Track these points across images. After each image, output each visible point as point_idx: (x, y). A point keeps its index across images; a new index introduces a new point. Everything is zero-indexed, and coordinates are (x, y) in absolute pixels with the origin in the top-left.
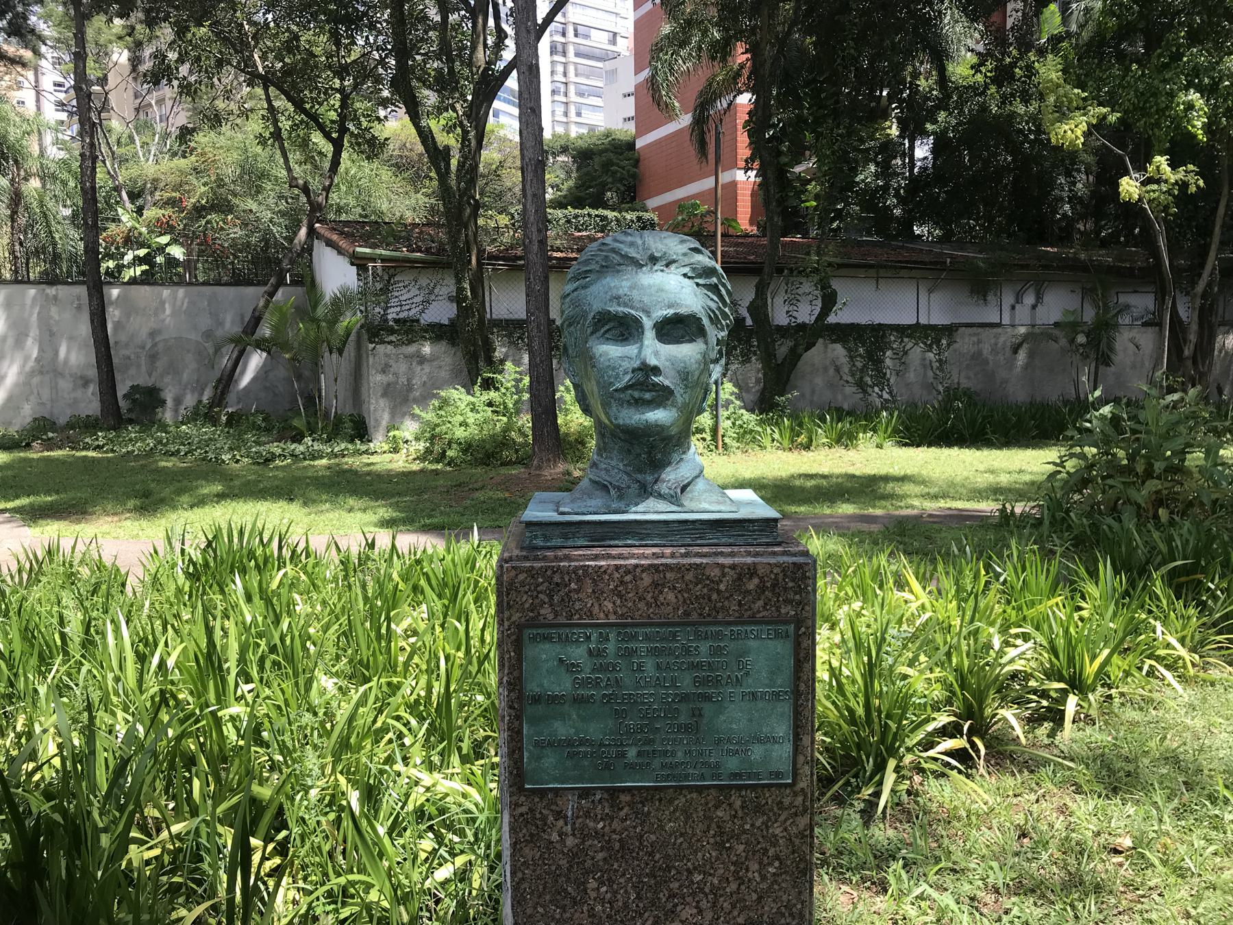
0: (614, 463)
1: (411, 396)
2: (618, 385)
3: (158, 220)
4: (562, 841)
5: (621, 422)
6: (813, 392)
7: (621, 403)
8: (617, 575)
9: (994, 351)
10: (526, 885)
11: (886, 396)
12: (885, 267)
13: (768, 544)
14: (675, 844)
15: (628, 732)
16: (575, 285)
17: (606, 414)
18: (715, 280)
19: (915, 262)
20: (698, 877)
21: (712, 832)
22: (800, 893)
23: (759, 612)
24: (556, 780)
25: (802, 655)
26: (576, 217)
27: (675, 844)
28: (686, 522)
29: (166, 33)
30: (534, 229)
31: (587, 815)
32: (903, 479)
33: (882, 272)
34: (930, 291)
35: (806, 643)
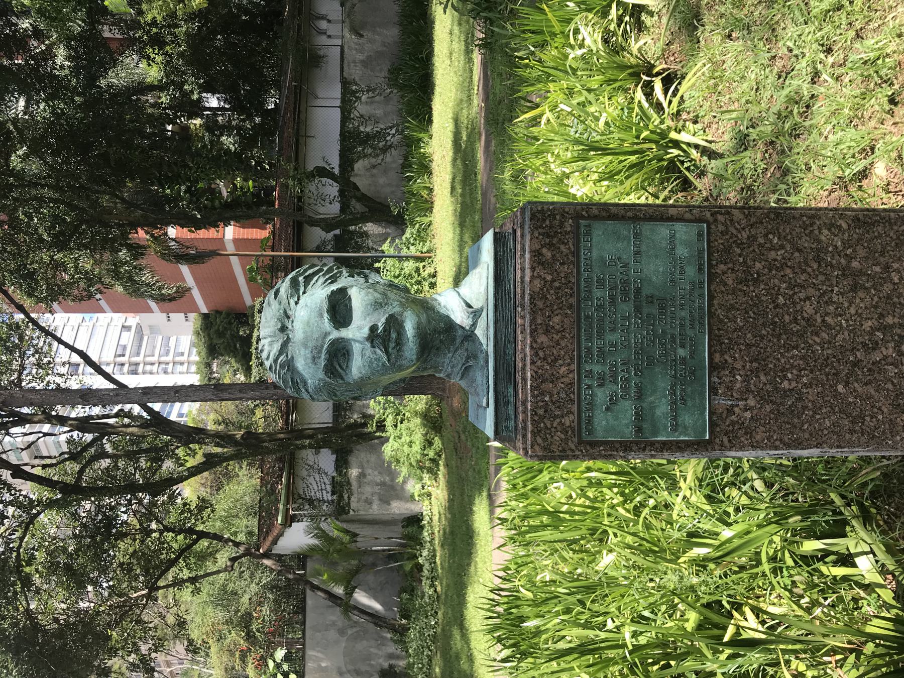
0: (447, 361)
2: (385, 359)
3: (256, 667)
4: (751, 409)
5: (415, 357)
6: (389, 185)
7: (399, 356)
8: (539, 363)
9: (361, 51)
10: (786, 439)
11: (393, 131)
12: (298, 130)
13: (515, 240)
14: (754, 318)
15: (665, 355)
16: (303, 390)
17: (407, 368)
18: (301, 279)
19: (295, 109)
20: (781, 300)
22: (794, 218)
25: (604, 214)
27: (754, 318)
28: (496, 306)
30: (266, 392)
31: (730, 388)
32: (456, 121)
33: (302, 133)
34: (317, 97)
35: (595, 211)
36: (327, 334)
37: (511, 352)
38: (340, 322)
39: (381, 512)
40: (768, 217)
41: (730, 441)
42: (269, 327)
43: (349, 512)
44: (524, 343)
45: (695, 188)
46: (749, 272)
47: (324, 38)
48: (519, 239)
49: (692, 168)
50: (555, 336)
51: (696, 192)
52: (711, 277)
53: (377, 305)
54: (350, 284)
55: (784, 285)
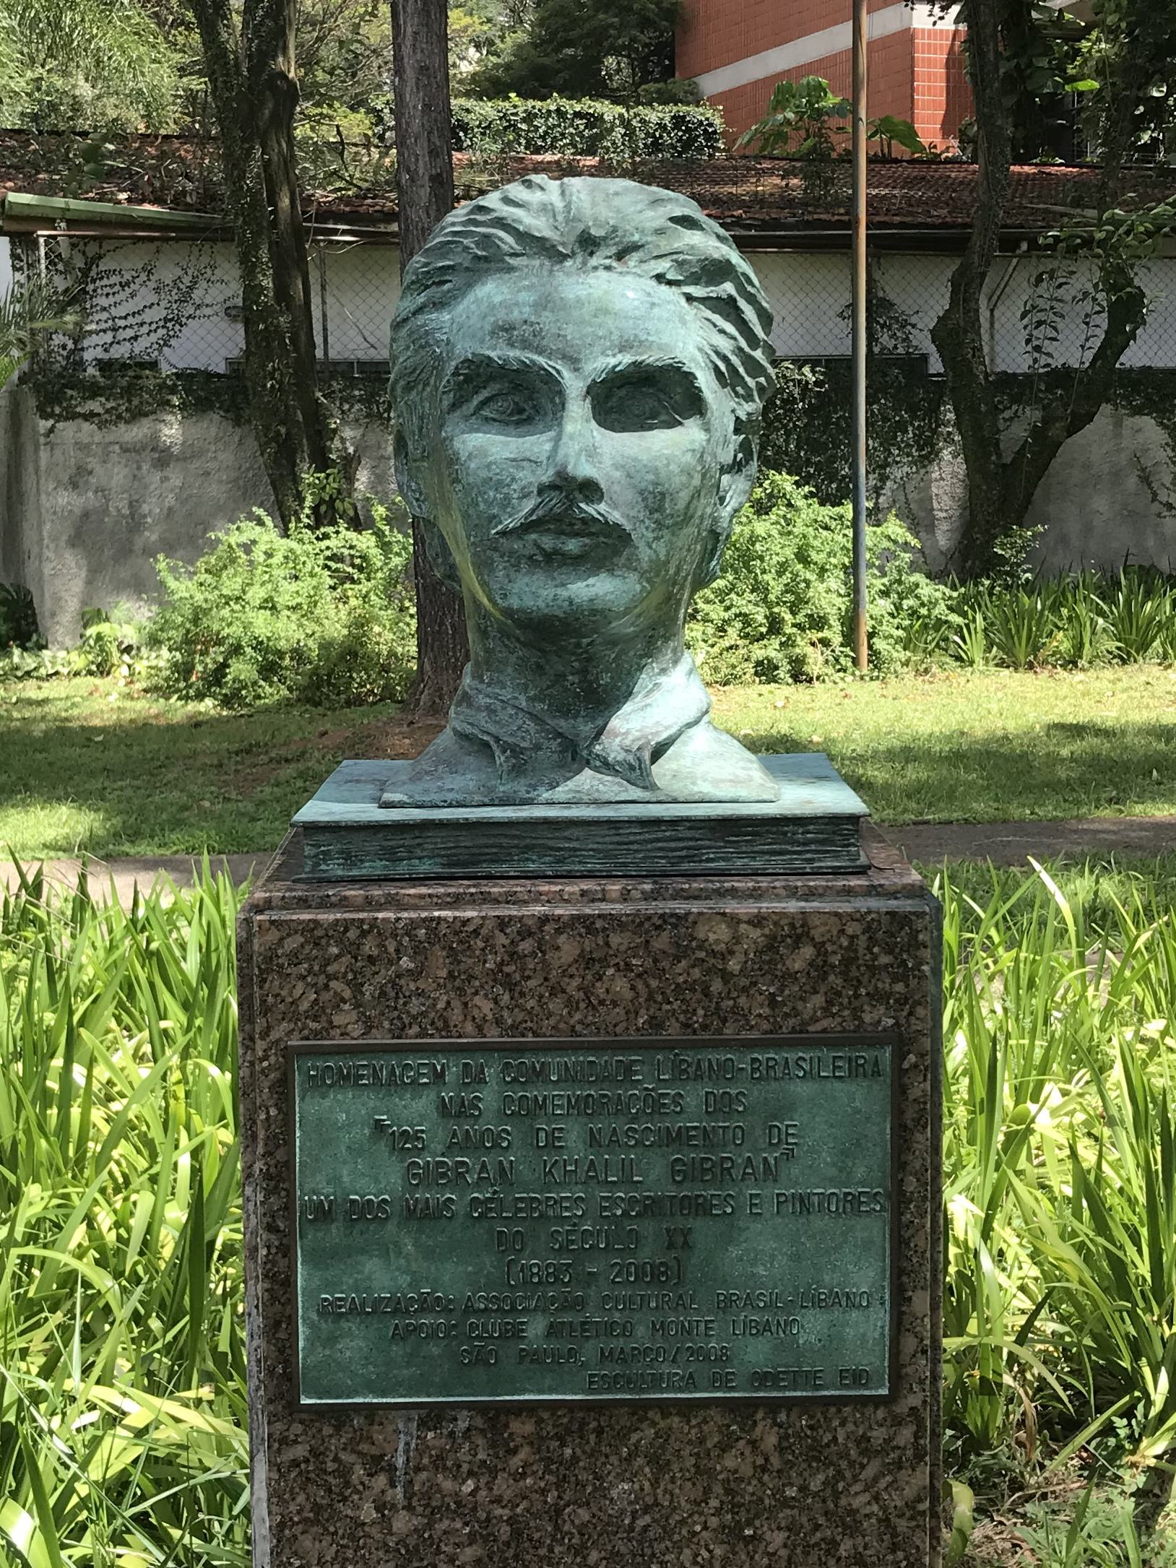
0: (506, 694)
1: (139, 543)
2: (509, 523)
4: (385, 1522)
5: (515, 603)
6: (1088, 529)
7: (516, 562)
8: (501, 939)
13: (836, 872)
14: (631, 1528)
15: (526, 1283)
16: (421, 299)
17: (484, 584)
18: (728, 288)
21: (714, 1503)
25: (910, 1114)
26: (530, 117)
27: (631, 1528)
28: (656, 822)
30: (421, 149)
31: (439, 1463)
35: (918, 1088)
36: (574, 363)
37: (532, 866)
38: (608, 397)
39: (47, 517)
41: (295, 1463)
42: (594, 204)
43: (45, 416)
44: (559, 900)
45: (1051, 1454)
46: (757, 1516)
49: (1112, 1442)
50: (576, 982)
51: (1037, 1455)
52: (742, 1410)
53: (655, 500)
54: (715, 423)
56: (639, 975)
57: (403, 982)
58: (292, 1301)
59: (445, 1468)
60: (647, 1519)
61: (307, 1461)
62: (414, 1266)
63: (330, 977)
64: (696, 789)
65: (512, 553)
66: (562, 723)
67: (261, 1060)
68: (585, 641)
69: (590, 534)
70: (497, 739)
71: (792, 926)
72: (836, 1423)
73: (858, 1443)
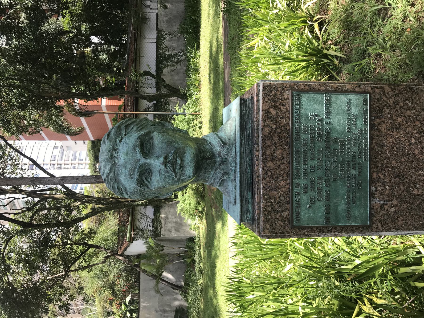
0: (211, 176)
1: (180, 222)
2: (174, 176)
4: (395, 206)
5: (192, 174)
6: (179, 80)
7: (182, 174)
8: (268, 179)
9: (166, 15)
10: (416, 225)
11: (182, 54)
12: (136, 53)
13: (253, 103)
14: (397, 152)
17: (187, 181)
20: (413, 140)
21: (391, 133)
23: (286, 109)
24: (366, 209)
25: (307, 88)
27: (397, 152)
28: (241, 144)
29: (51, 306)
33: (138, 55)
34: (145, 38)
36: (138, 161)
38: (146, 153)
40: (406, 90)
41: (382, 226)
42: (104, 155)
43: (160, 236)
46: (394, 123)
47: (149, 9)
48: (255, 102)
50: (277, 162)
55: (415, 132)
56: (276, 148)
57: (277, 201)
58: (347, 226)
59: (383, 192)
60: (395, 148)
61: (381, 223)
62: (340, 199)
63: (276, 218)
64: (233, 135)
65: (180, 175)
66: (217, 164)
67: (294, 233)
68: (200, 159)
69: (176, 158)
70: (221, 178)
71: (265, 113)
72: (374, 106)
73: (379, 101)
